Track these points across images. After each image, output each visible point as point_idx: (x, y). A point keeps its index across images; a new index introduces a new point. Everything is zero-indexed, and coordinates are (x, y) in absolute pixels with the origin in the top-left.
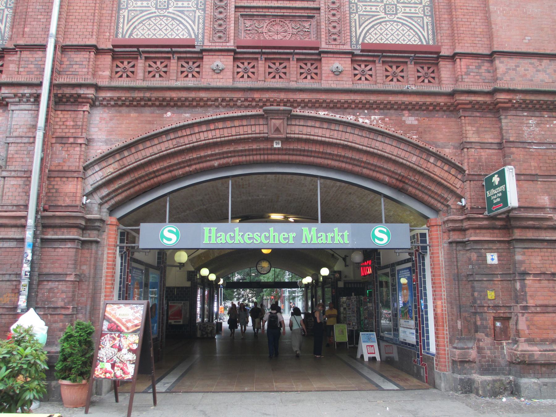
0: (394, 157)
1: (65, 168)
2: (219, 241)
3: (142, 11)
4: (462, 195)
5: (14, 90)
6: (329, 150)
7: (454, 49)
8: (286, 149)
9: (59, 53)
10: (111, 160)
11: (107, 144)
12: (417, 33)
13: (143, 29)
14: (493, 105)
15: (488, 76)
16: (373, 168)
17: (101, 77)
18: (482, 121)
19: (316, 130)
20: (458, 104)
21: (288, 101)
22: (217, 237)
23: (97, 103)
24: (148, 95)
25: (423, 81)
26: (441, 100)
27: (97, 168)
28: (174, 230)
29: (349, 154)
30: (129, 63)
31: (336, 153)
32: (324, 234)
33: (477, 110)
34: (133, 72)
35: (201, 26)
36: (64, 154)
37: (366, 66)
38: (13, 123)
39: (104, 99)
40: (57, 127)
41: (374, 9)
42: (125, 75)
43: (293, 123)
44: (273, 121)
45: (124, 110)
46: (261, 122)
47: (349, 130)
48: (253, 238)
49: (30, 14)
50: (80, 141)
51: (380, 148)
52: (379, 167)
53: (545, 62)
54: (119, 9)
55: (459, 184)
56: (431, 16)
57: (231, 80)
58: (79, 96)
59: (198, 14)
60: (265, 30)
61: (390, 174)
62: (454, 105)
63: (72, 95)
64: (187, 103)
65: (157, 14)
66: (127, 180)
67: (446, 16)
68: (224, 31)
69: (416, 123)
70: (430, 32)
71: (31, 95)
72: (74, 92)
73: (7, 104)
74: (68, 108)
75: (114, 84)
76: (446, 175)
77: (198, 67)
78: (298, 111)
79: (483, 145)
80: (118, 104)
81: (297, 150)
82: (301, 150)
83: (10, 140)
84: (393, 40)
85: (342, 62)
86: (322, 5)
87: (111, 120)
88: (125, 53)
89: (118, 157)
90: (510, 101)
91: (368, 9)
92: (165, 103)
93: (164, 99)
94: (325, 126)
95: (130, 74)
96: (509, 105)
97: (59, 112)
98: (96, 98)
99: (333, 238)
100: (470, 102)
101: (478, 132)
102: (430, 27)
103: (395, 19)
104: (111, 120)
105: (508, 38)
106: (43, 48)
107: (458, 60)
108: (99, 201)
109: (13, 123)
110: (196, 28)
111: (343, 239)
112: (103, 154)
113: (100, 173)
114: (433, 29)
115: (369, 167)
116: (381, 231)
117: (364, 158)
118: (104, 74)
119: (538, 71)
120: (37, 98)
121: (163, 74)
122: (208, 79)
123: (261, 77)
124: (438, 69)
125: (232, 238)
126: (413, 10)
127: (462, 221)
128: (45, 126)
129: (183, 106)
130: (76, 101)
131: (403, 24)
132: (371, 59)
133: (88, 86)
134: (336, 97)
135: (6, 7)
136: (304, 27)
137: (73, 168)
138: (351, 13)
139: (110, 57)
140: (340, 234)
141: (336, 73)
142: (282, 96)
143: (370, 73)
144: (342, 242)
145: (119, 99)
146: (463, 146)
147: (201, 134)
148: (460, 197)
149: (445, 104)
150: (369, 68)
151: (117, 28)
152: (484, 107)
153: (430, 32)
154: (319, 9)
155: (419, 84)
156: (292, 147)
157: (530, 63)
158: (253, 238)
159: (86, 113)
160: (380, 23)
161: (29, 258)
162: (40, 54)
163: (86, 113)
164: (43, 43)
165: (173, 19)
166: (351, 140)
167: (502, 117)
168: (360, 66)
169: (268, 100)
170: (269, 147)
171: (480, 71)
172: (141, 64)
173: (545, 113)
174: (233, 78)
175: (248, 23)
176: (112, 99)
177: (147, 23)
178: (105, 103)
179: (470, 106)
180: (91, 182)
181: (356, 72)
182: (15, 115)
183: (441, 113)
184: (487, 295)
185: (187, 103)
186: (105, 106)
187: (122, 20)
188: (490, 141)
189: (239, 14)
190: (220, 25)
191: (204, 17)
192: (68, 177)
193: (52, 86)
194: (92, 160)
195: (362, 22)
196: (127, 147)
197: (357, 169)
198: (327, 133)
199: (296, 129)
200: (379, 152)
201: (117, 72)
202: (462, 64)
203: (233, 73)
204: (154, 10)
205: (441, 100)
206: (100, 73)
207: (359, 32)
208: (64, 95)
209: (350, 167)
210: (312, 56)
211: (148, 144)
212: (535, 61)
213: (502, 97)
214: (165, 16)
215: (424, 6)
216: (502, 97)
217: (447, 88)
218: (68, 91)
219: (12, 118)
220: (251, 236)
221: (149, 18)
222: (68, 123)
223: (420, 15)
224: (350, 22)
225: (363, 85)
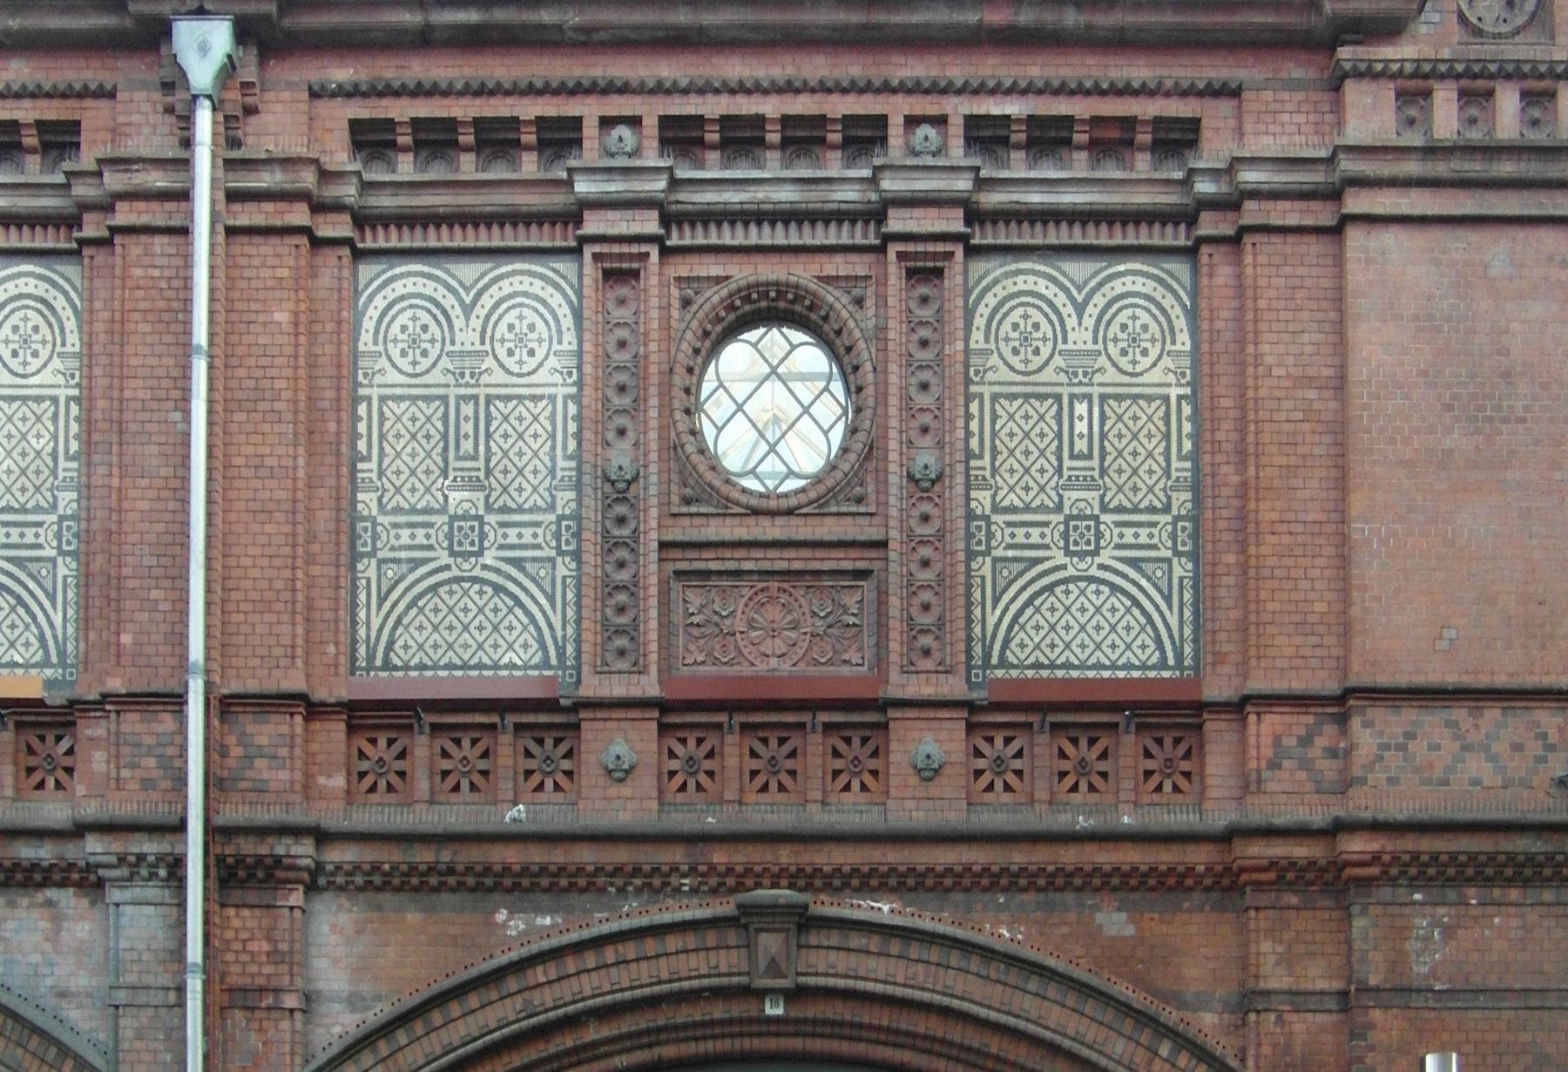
6: (905, 1022)
15: (1329, 768)
26: (1199, 857)
47: (955, 958)
53: (1493, 713)
62: (1227, 875)
68: (632, 631)
79: (1300, 999)
100: (1273, 864)
105: (1398, 644)
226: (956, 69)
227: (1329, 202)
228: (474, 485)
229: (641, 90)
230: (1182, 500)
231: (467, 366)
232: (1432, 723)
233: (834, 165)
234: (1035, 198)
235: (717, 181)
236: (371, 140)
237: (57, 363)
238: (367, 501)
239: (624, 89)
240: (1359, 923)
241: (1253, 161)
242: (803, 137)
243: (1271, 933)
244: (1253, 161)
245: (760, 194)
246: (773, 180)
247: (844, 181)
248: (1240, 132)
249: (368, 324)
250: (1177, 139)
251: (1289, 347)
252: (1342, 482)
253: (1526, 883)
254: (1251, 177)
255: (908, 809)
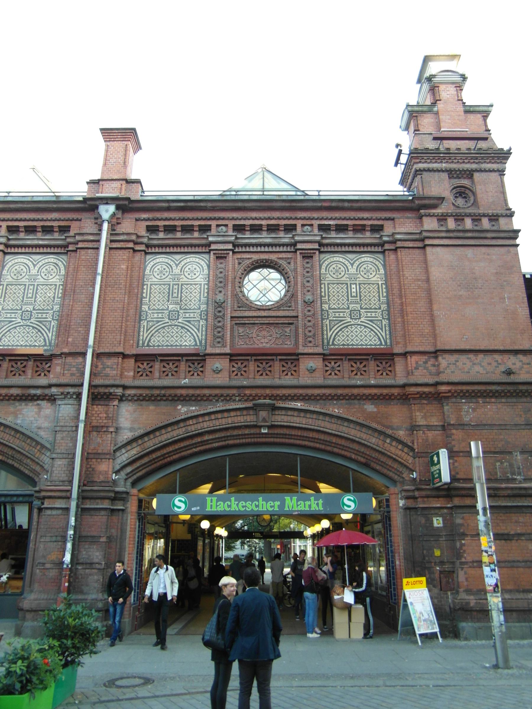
0: (357, 439)
1: (100, 451)
2: (219, 509)
3: (158, 322)
4: (413, 469)
5: (61, 390)
6: (305, 434)
7: (406, 347)
8: (271, 434)
9: (95, 359)
10: (134, 445)
11: (131, 431)
12: (376, 334)
13: (159, 337)
14: (436, 395)
15: (433, 370)
16: (341, 447)
17: (126, 377)
18: (428, 407)
19: (295, 418)
20: (409, 394)
21: (273, 395)
22: (217, 506)
23: (124, 399)
24: (163, 392)
25: (382, 374)
26: (396, 391)
27: (123, 451)
28: (183, 500)
29: (322, 437)
30: (148, 364)
31: (311, 436)
32: (302, 502)
33: (424, 398)
34: (151, 372)
35: (204, 333)
36: (99, 440)
37: (335, 363)
38: (60, 415)
39: (129, 395)
40: (93, 418)
41: (342, 315)
42: (144, 374)
43: (277, 413)
44: (261, 412)
45: (144, 403)
46: (251, 412)
47: (321, 417)
48: (246, 506)
49: (73, 327)
50: (111, 429)
51: (346, 432)
52: (346, 447)
53: (481, 356)
54: (140, 320)
55: (411, 460)
56: (389, 319)
57: (228, 379)
58: (111, 394)
59: (201, 323)
60: (254, 335)
61: (355, 452)
62: (405, 396)
63: (105, 393)
64: (193, 398)
65: (170, 323)
66: (146, 460)
67: (400, 320)
68: (223, 337)
69: (375, 410)
70: (387, 332)
71: (74, 393)
72: (107, 391)
73: (55, 400)
74: (102, 403)
75: (137, 383)
76: (400, 453)
77: (202, 367)
78: (281, 404)
79: (430, 427)
80: (139, 399)
81: (280, 434)
82: (283, 434)
83: (58, 429)
84: (357, 340)
85: (316, 362)
86: (300, 314)
87: (134, 412)
88: (145, 359)
89: (140, 442)
90: (450, 391)
91: (337, 315)
92: (176, 398)
93: (176, 395)
94: (302, 414)
95: (148, 373)
96: (450, 394)
97: (95, 406)
98: (123, 395)
99: (310, 506)
100: (418, 393)
101: (425, 417)
102: (387, 328)
103: (359, 323)
104: (134, 412)
105: (450, 338)
106: (84, 354)
107: (409, 357)
108: (125, 477)
109: (60, 415)
110: (200, 335)
111: (318, 506)
112: (129, 440)
113: (126, 455)
114: (390, 330)
115: (339, 446)
116: (349, 500)
117: (334, 440)
118: (129, 374)
119: (474, 364)
120: (79, 396)
121: (174, 373)
122: (211, 379)
123: (252, 377)
124: (394, 364)
125: (229, 506)
126: (373, 315)
127: (413, 491)
128: (86, 418)
129: (190, 400)
130: (108, 397)
131: (365, 327)
132: (339, 357)
133: (117, 386)
134: (310, 392)
135: (53, 319)
136: (286, 332)
137: (106, 451)
138: (323, 319)
139: (133, 360)
140: (316, 502)
141: (310, 372)
142: (268, 391)
143: (338, 369)
144: (317, 509)
145: (141, 395)
146: (413, 428)
147: (205, 423)
148: (412, 471)
149: (399, 394)
150: (337, 364)
151: (139, 336)
152: (430, 396)
153: (387, 332)
154: (297, 317)
155: (378, 377)
156: (276, 432)
157: (468, 358)
158: (246, 506)
159: (116, 407)
160: (347, 327)
161: (73, 524)
162: (80, 359)
163: (116, 407)
164: (83, 350)
165: (182, 327)
166: (322, 425)
167: (445, 404)
168: (330, 363)
169: (256, 395)
170: (258, 432)
171: (427, 366)
172: (157, 365)
173: (480, 399)
174: (230, 376)
175: (241, 330)
176: (135, 395)
177: (161, 331)
178: (130, 398)
179: (418, 396)
180: (119, 462)
181: (327, 368)
182: (61, 409)
183: (395, 401)
184: (434, 552)
185: (193, 398)
186: (130, 400)
187: (142, 329)
188: (436, 424)
189: (234, 322)
190: (219, 332)
191: (207, 326)
192: (101, 459)
193: (90, 386)
194: (120, 445)
195: (332, 326)
196: (147, 434)
197: (329, 448)
198: (304, 421)
199: (279, 418)
200: (346, 435)
201: (138, 372)
202: (413, 360)
203: (230, 372)
204: (167, 320)
205: (396, 391)
206: (126, 373)
207: (329, 334)
208: (99, 393)
209: (323, 447)
210: (292, 358)
211: (163, 431)
212: (471, 356)
213: (443, 388)
214: (176, 325)
215: (382, 311)
216: (443, 388)
217: (401, 381)
218: (102, 390)
219: (59, 411)
220: (244, 504)
221: (163, 327)
222: (101, 415)
223: (379, 318)
224: (322, 327)
225: (333, 381)
226: (315, 215)
227: (421, 242)
228: (177, 304)
229: (228, 219)
230: (384, 307)
231: (176, 278)
232: (463, 358)
233: (282, 234)
234: (338, 241)
235: (248, 237)
236: (151, 229)
237: (57, 277)
238: (145, 308)
239: (224, 219)
240: (446, 408)
241: (399, 233)
242: (273, 229)
243: (419, 410)
244: (399, 233)
245: (261, 240)
246: (265, 237)
247: (285, 238)
248: (395, 227)
249: (148, 268)
250: (377, 229)
251: (411, 272)
252: (430, 302)
253: (496, 397)
254: (398, 237)
255: (305, 379)
